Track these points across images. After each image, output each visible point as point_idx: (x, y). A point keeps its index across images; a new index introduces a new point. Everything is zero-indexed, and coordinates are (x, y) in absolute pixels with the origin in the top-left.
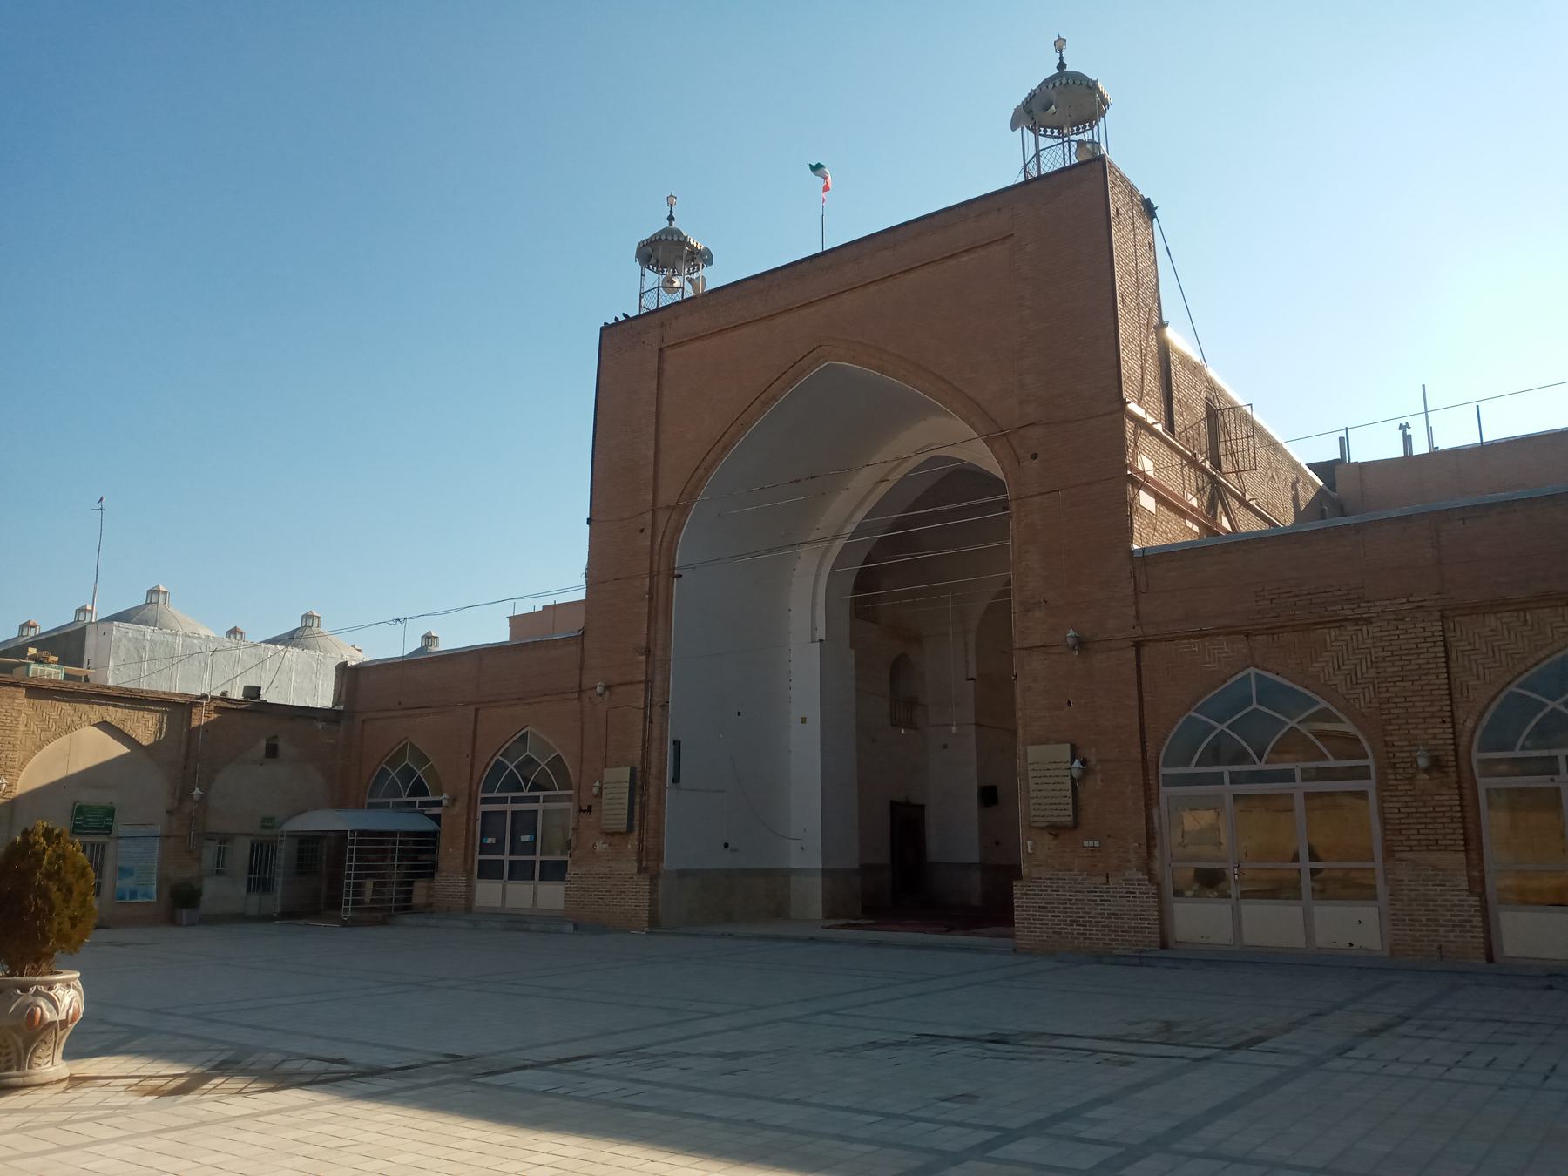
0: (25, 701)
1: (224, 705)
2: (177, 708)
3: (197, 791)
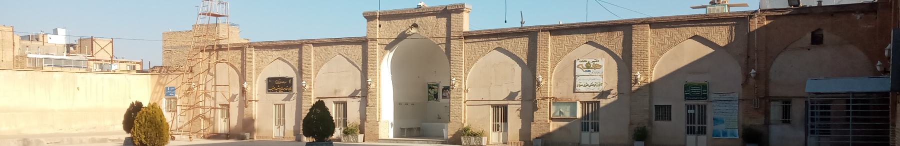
2: (740, 21)
3: (753, 71)
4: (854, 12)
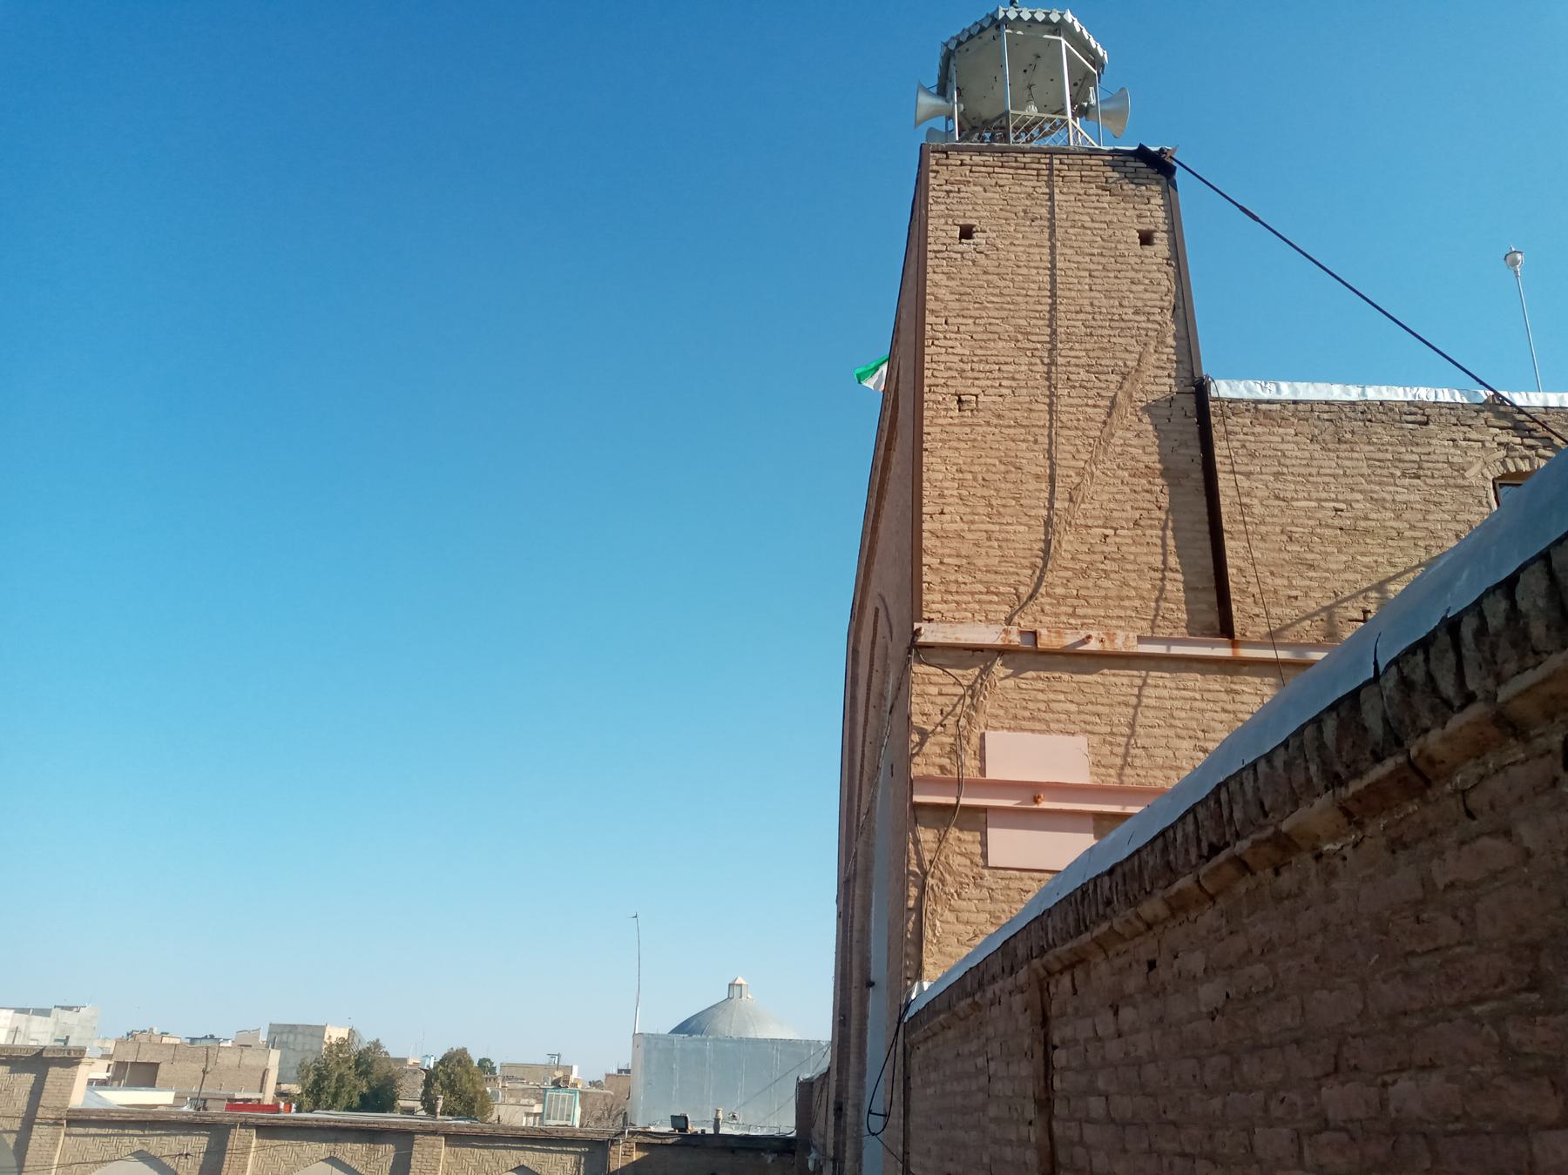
0: (444, 1150)
1: (651, 1144)
4: (763, 1150)
